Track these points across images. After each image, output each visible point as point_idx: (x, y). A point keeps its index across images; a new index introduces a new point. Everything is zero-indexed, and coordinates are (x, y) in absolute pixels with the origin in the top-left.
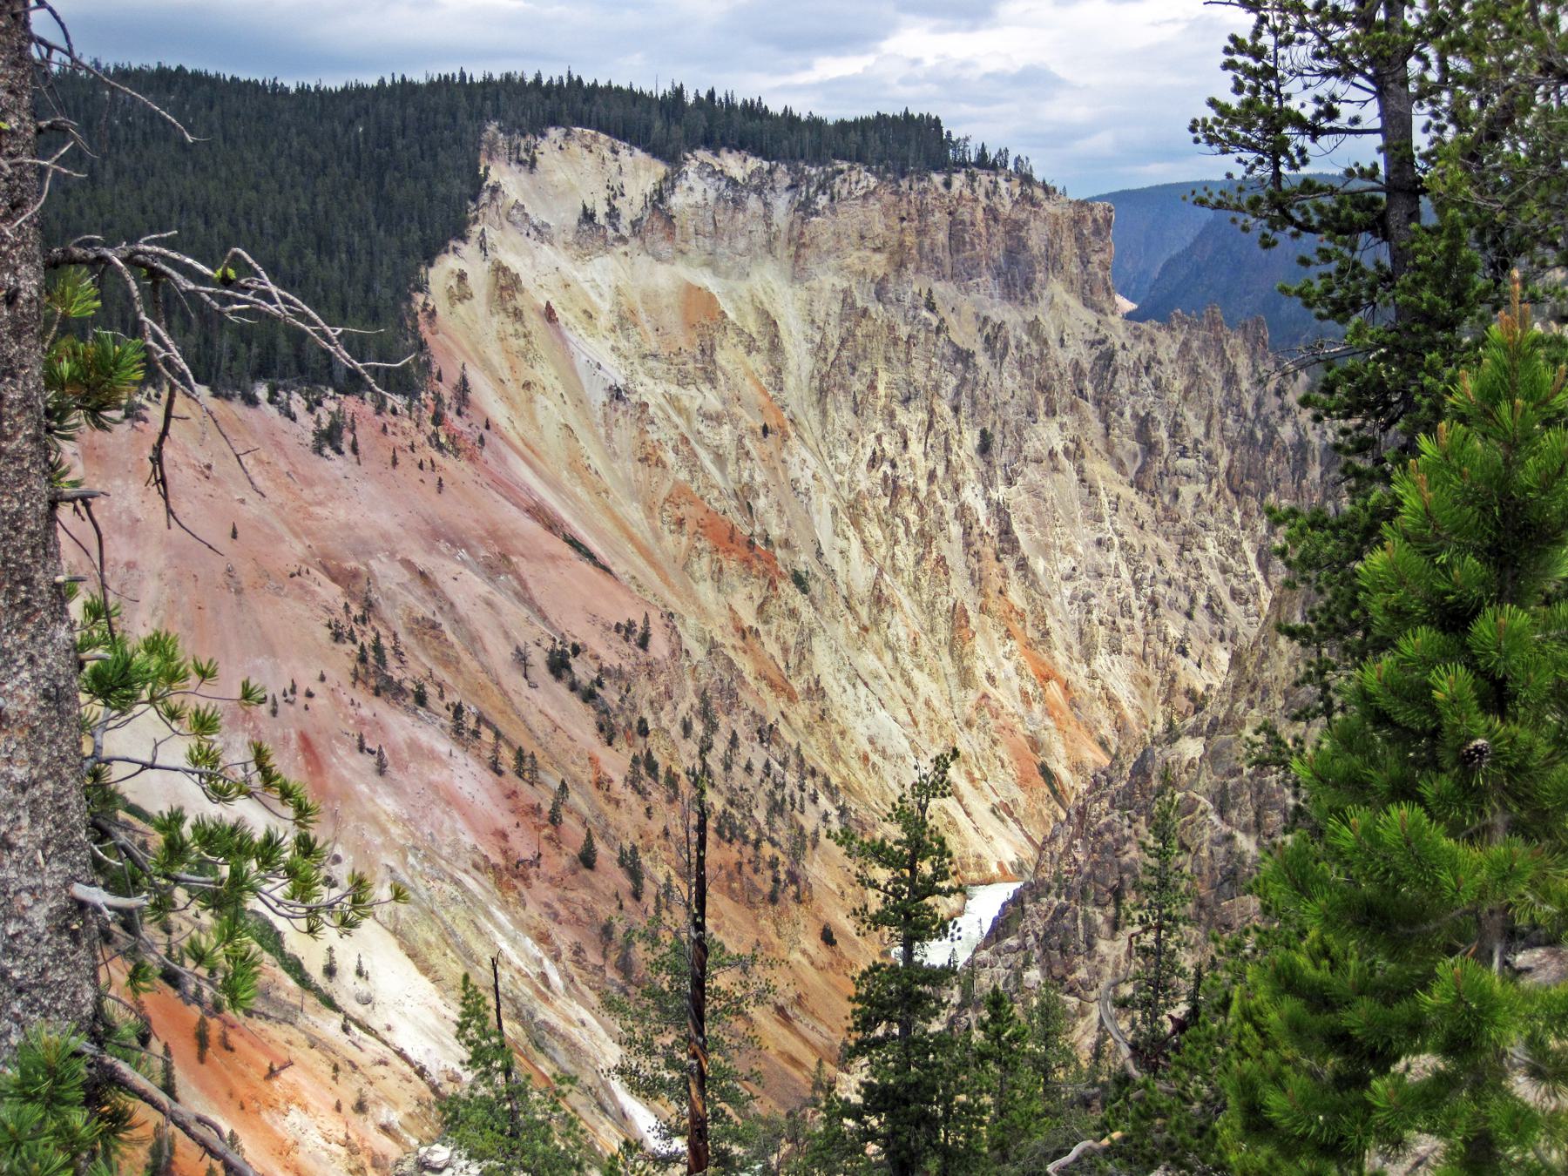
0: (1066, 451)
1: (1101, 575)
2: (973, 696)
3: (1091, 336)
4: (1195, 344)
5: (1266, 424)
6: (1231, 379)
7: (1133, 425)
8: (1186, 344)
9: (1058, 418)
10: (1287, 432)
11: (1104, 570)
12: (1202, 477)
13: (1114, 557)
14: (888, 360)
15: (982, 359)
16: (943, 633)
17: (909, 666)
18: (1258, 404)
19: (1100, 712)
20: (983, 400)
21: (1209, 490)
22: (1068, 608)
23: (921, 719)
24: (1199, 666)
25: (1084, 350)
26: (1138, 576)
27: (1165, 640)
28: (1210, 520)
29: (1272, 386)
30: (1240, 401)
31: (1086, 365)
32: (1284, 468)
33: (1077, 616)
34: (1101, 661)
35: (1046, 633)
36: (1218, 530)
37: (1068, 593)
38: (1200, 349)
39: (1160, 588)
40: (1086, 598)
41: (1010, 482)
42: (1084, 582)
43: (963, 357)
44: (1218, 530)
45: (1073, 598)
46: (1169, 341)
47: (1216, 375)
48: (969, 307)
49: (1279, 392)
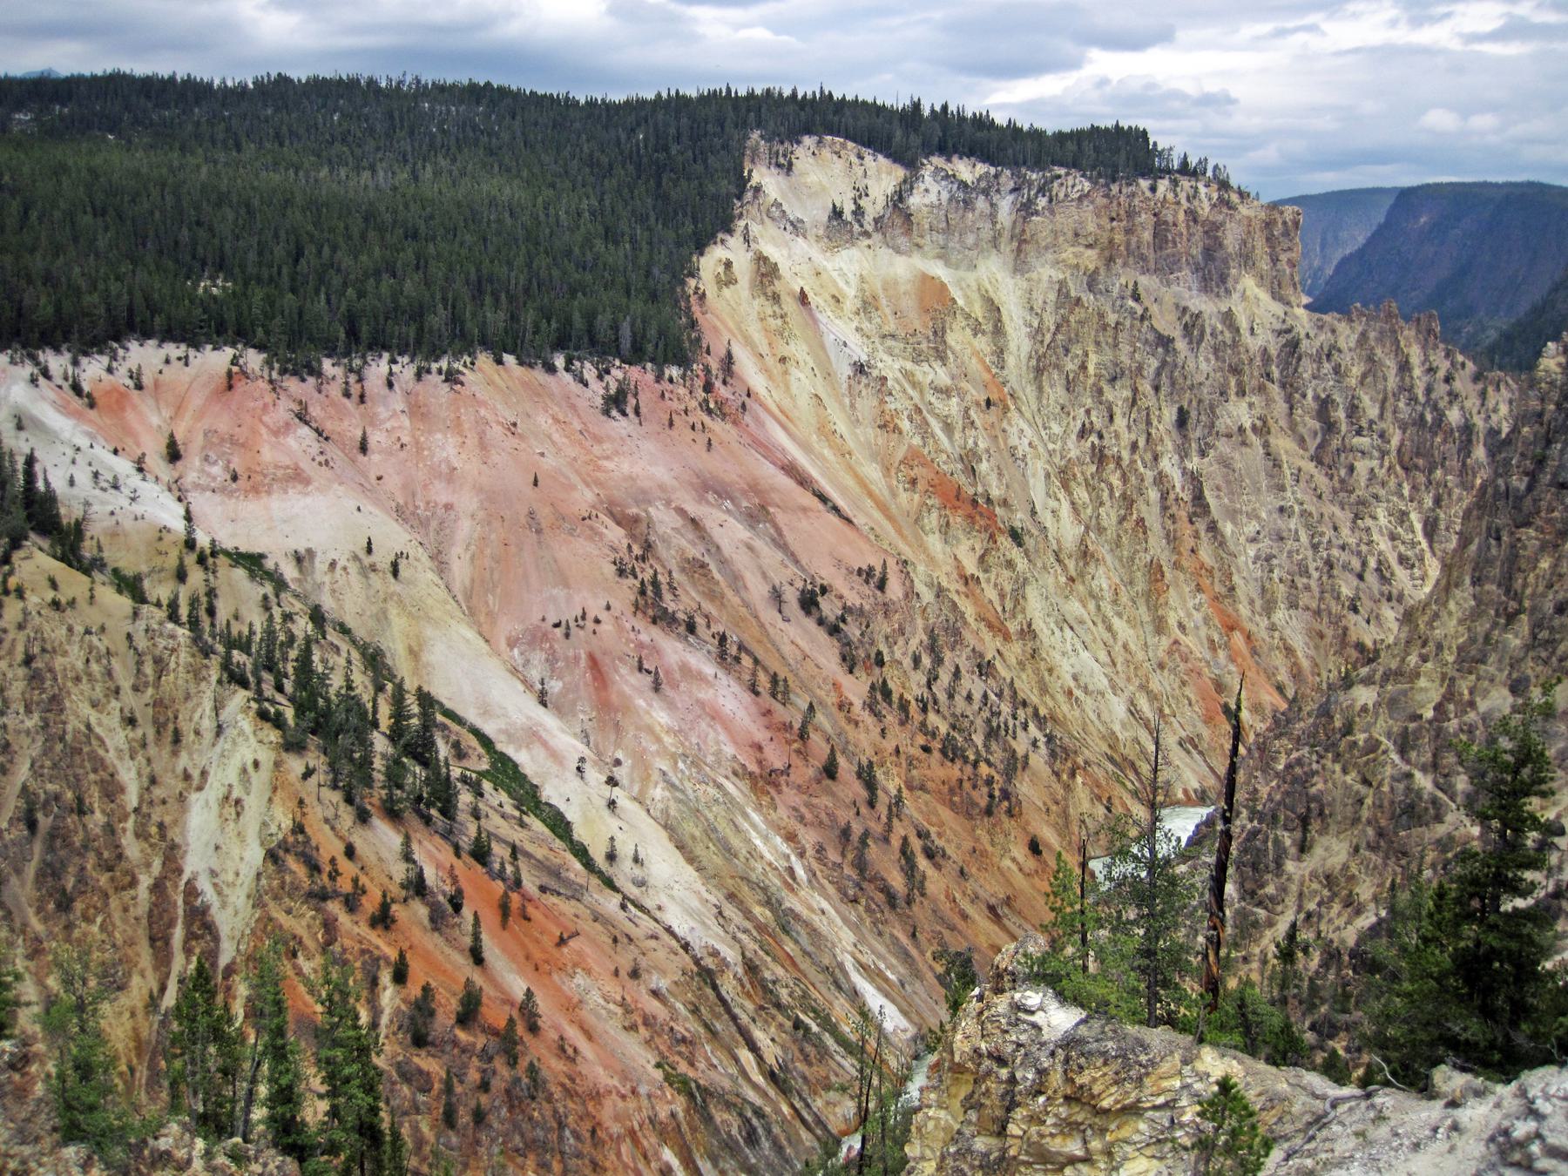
0: (1254, 428)
1: (1282, 539)
2: (1165, 642)
3: (1278, 326)
4: (1372, 335)
5: (1435, 408)
7: (1314, 405)
8: (1364, 335)
9: (1247, 399)
10: (1454, 416)
11: (1285, 534)
12: (1376, 454)
14: (1098, 343)
15: (1181, 345)
16: (1141, 585)
17: (1110, 614)
18: (1429, 390)
19: (1279, 661)
20: (1181, 381)
21: (1382, 466)
22: (1251, 566)
23: (1119, 660)
24: (1368, 622)
25: (1271, 337)
26: (1316, 540)
27: (1338, 598)
28: (1382, 492)
29: (1441, 374)
30: (1412, 387)
31: (1273, 352)
32: (1452, 448)
33: (1259, 574)
34: (1280, 615)
35: (1232, 589)
36: (1388, 501)
37: (1252, 553)
38: (1377, 339)
39: (1335, 552)
40: (1268, 559)
41: (1203, 454)
42: (1266, 545)
43: (1165, 342)
44: (1388, 501)
45: (1257, 558)
46: (1348, 331)
47: (1391, 365)
49: (1448, 379)
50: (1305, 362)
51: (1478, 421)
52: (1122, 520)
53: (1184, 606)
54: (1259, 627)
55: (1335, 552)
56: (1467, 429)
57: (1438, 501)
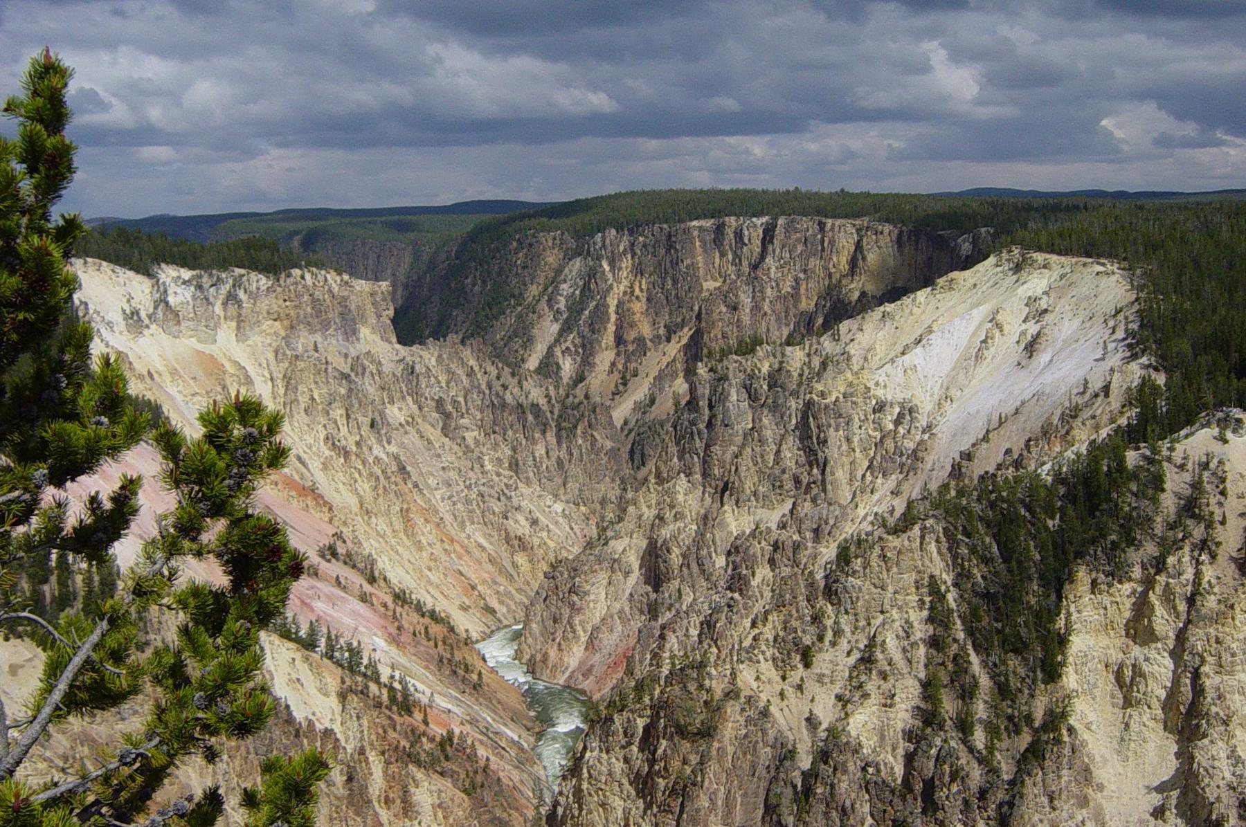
0: (407, 422)
5: (497, 395)
6: (471, 373)
8: (440, 356)
10: (508, 398)
13: (453, 475)
14: (316, 383)
16: (398, 525)
18: (490, 387)
19: (477, 552)
28: (485, 450)
34: (469, 529)
35: (442, 519)
37: (438, 497)
39: (481, 488)
43: (346, 377)
45: (443, 499)
48: (333, 348)
49: (498, 378)
50: (421, 378)
51: (522, 400)
52: (375, 488)
53: (427, 533)
55: (481, 488)
56: (520, 405)
57: (514, 450)
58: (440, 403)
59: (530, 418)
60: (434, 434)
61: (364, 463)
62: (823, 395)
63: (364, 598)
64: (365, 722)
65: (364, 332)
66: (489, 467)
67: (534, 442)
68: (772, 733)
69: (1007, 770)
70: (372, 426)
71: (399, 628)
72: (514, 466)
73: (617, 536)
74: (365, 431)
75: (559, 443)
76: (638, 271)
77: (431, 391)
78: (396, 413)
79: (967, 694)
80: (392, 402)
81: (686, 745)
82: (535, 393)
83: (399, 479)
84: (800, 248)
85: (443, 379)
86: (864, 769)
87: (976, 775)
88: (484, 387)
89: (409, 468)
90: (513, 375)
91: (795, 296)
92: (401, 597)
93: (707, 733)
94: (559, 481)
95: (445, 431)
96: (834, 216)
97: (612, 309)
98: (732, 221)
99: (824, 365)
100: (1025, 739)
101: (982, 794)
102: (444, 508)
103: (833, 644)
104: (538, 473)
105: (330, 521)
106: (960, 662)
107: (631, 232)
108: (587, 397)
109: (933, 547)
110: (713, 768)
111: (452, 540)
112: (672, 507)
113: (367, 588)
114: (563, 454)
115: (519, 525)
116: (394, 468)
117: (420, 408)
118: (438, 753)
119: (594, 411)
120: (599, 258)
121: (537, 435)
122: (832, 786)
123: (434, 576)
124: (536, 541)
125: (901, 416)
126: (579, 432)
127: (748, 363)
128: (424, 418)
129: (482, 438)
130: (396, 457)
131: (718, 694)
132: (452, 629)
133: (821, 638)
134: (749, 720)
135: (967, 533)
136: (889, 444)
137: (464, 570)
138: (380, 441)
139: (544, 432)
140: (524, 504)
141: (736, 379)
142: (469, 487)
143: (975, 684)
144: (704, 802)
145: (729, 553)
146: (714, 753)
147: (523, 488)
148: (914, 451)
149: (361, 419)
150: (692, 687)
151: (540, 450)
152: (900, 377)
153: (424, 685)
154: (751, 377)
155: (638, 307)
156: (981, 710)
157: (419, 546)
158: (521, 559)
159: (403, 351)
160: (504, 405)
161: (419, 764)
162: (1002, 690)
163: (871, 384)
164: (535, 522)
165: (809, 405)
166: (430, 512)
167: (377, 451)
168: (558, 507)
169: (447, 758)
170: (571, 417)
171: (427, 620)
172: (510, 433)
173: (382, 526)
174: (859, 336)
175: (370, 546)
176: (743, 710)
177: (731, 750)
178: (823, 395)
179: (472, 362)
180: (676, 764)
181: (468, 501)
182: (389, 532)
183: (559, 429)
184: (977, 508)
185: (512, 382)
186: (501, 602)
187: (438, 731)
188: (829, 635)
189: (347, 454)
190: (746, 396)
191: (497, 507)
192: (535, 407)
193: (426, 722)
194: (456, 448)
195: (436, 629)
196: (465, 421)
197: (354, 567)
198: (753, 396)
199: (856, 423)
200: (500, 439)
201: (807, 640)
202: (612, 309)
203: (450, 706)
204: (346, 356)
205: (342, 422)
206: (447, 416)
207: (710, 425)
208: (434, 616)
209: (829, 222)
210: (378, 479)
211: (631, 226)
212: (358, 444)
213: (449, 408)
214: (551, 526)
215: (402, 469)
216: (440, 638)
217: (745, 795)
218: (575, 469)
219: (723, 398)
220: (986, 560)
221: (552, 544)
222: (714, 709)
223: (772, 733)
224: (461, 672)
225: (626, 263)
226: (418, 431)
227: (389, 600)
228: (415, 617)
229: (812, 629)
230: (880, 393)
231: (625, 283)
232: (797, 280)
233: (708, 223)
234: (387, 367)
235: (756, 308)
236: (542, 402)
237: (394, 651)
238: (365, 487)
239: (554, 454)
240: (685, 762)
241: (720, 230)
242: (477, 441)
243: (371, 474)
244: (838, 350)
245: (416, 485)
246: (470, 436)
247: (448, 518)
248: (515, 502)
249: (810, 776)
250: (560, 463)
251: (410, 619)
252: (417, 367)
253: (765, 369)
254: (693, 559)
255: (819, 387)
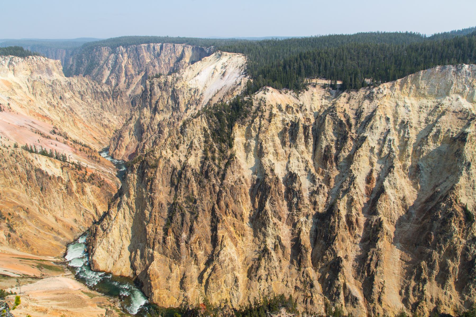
2: (81, 131)
6: (87, 84)
7: (77, 93)
8: (78, 80)
10: (99, 90)
13: (86, 111)
16: (72, 123)
18: (93, 87)
19: (95, 129)
31: (67, 85)
34: (92, 124)
40: (86, 116)
42: (84, 114)
43: (51, 86)
48: (46, 77)
52: (64, 115)
53: (80, 125)
54: (90, 126)
56: (102, 92)
57: (102, 103)
58: (79, 92)
59: (105, 95)
60: (80, 101)
61: (60, 108)
62: (177, 87)
63: (65, 143)
64: (69, 174)
65: (54, 73)
66: (95, 108)
67: (107, 101)
68: (171, 165)
69: (223, 167)
70: (61, 98)
71: (76, 149)
72: (102, 107)
73: (131, 123)
74: (59, 100)
75: (113, 101)
76: (129, 57)
77: (76, 89)
78: (67, 95)
79: (213, 152)
80: (66, 92)
81: (151, 170)
82: (106, 89)
83: (71, 112)
84: (169, 51)
85: (80, 86)
86: (192, 170)
87: (216, 169)
88: (91, 87)
89: (73, 109)
90: (99, 84)
91: (169, 63)
92: (75, 142)
93: (156, 166)
94: (114, 110)
95: (82, 99)
96: (177, 43)
97: (123, 67)
98: (152, 45)
99: (177, 80)
100: (226, 161)
101: (218, 173)
102: (84, 119)
103: (183, 144)
104: (109, 109)
105: (52, 124)
106: (211, 146)
107: (126, 47)
108: (119, 89)
109: (204, 121)
110: (158, 174)
111: (88, 127)
112: (143, 115)
113: (66, 140)
114: (115, 104)
115: (106, 122)
116: (69, 109)
117: (74, 94)
118: (90, 178)
119: (122, 92)
120: (119, 54)
121: (107, 99)
122: (186, 175)
123: (84, 136)
124: (110, 125)
125: (195, 91)
126: (118, 98)
127: (159, 80)
128: (76, 96)
129: (92, 101)
130: (69, 107)
131: (158, 158)
132: (90, 149)
133: (180, 143)
134: (165, 162)
135: (211, 117)
136: (193, 98)
137: (92, 134)
138: (64, 103)
139: (109, 98)
140: (107, 116)
141: (156, 84)
142: (91, 113)
143: (215, 150)
144: (157, 182)
145: (158, 125)
146: (158, 170)
147: (105, 112)
148: (199, 99)
149: (57, 97)
150: (151, 156)
151: (109, 103)
152: (195, 82)
153: (84, 163)
154: (160, 83)
155: (130, 66)
156: (217, 155)
157: (79, 129)
158: (107, 130)
159: (67, 79)
160: (97, 92)
161: (85, 182)
162: (221, 151)
163: (188, 84)
164: (109, 121)
165: (174, 89)
166: (81, 120)
167: (63, 105)
168: (115, 117)
169: (93, 180)
170: (116, 94)
171: (84, 147)
172: (100, 99)
173: (68, 124)
174: (184, 73)
175: (65, 130)
176: (164, 160)
177: (162, 169)
178: (177, 87)
179: (87, 81)
180: (149, 174)
181: (91, 117)
182: (70, 126)
183: (113, 98)
184: (213, 111)
185: (99, 86)
186: (103, 141)
187: (89, 173)
188: (182, 142)
189: (54, 106)
190: (159, 88)
191: (99, 118)
192: (106, 92)
193: (86, 172)
194: (86, 104)
195: (86, 149)
196: (87, 97)
197: (61, 135)
198: (160, 88)
199: (185, 93)
200: (97, 101)
201: (177, 143)
202: (123, 67)
203: (92, 167)
204: (50, 80)
205: (52, 98)
206: (82, 95)
207: (151, 95)
208: (85, 146)
209: (176, 45)
210: (64, 112)
211: (126, 45)
212: (57, 104)
213: (82, 93)
214: (114, 122)
215: (71, 109)
216: (87, 151)
217: (166, 179)
218: (118, 108)
219: (153, 89)
220: (215, 123)
221: (115, 126)
222: (157, 161)
223: (171, 165)
224: (94, 159)
225: (126, 55)
226: (74, 100)
227: (72, 143)
228: (80, 146)
229: (178, 141)
230: (190, 86)
231: (126, 60)
232: (169, 59)
233: (146, 45)
234: (63, 83)
235: (160, 67)
236: (107, 91)
237: (75, 155)
238: (61, 115)
239: (112, 104)
240: (151, 173)
241: (149, 46)
242: (91, 102)
243: (63, 111)
244: (180, 76)
245: (76, 113)
246: (89, 100)
247: (86, 122)
248: (104, 116)
249: (180, 174)
250: (114, 106)
251: (78, 147)
252: (72, 83)
253: (163, 81)
254: (150, 127)
255: (176, 85)
